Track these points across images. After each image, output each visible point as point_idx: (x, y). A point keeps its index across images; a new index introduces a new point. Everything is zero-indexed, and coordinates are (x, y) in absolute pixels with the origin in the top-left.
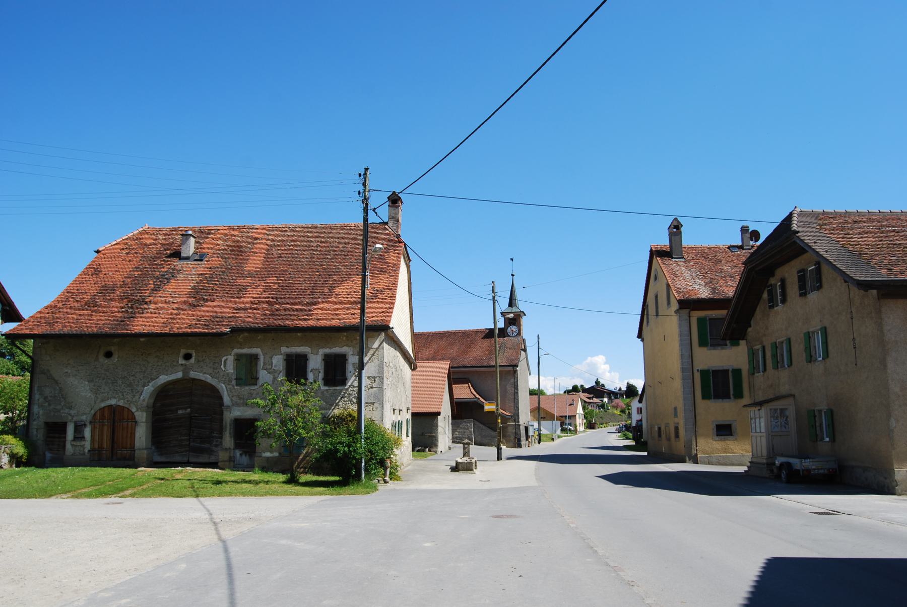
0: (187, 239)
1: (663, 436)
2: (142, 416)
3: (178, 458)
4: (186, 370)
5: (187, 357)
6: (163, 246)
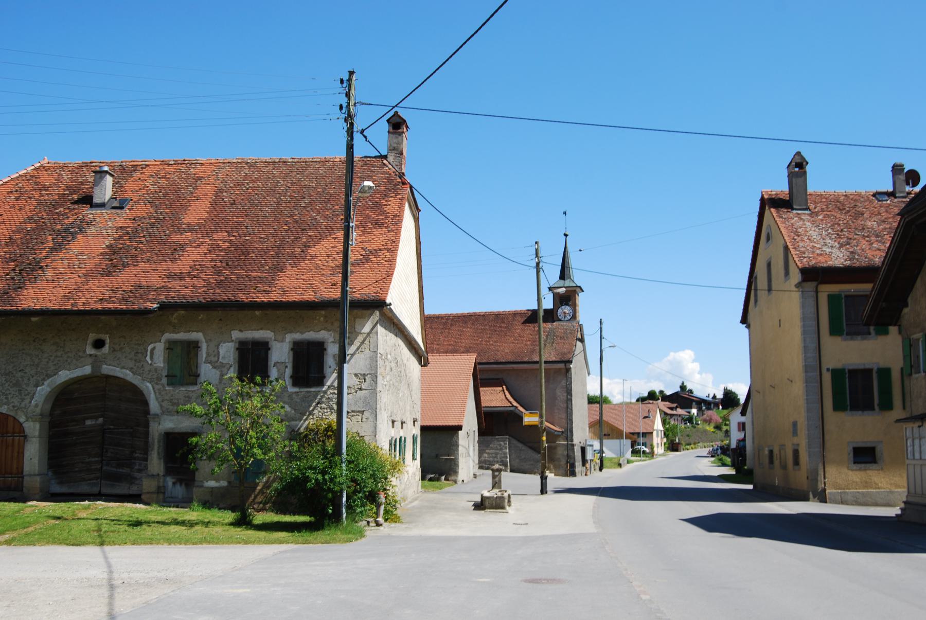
0: (102, 178)
1: (777, 462)
2: (33, 428)
3: (84, 488)
4: (96, 362)
5: (99, 344)
6: (68, 188)
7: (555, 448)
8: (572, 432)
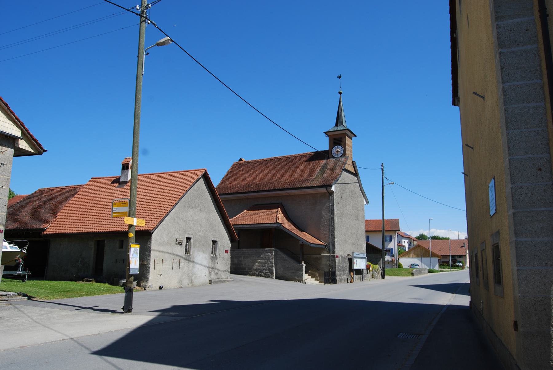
7: (320, 259)
8: (333, 245)
